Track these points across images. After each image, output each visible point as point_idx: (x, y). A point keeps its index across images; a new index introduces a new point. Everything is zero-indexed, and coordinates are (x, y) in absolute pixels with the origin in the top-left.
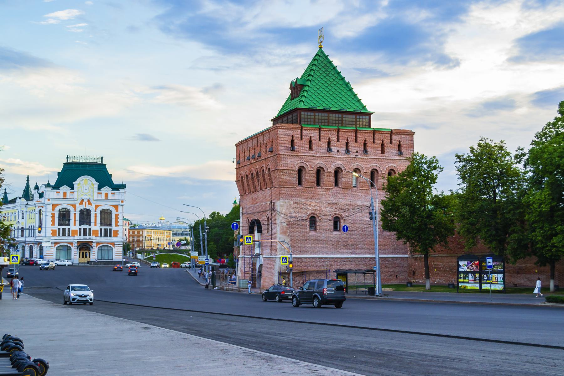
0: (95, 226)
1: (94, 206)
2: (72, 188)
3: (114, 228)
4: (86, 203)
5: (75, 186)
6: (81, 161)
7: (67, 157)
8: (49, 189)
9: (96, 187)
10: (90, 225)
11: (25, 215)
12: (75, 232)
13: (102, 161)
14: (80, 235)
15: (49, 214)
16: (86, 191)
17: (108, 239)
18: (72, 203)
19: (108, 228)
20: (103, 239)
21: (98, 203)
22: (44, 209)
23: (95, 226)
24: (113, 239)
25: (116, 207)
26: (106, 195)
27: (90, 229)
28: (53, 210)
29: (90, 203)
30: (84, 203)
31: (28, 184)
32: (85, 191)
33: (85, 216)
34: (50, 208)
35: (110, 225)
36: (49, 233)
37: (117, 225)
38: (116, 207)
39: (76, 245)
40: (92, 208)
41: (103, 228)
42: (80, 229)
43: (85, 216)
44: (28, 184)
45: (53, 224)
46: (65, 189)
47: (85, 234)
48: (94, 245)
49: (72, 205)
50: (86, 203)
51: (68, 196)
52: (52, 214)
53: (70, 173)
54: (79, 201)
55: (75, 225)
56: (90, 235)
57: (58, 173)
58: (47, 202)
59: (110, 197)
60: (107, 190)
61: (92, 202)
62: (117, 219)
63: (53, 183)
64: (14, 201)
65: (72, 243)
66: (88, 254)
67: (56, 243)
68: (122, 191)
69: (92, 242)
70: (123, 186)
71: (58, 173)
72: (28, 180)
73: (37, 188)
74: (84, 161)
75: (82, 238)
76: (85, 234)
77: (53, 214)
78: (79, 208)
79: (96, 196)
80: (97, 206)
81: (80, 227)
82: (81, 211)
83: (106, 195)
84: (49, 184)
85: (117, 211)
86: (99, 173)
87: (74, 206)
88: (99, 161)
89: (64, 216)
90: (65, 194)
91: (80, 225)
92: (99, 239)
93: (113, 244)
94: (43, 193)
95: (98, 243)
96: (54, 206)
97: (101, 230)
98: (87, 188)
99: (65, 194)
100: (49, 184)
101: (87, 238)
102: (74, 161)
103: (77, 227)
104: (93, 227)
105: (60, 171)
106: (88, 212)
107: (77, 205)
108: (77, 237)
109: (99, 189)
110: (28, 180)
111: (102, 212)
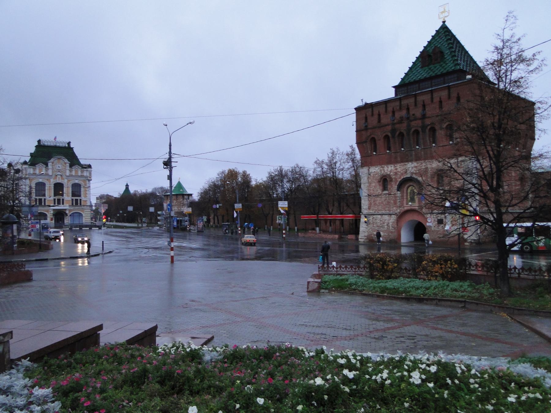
0: (67, 197)
2: (47, 165)
5: (50, 164)
7: (39, 141)
23: (67, 197)
27: (63, 199)
33: (58, 188)
35: (80, 196)
37: (86, 197)
39: (52, 212)
40: (65, 182)
43: (58, 188)
47: (59, 203)
53: (43, 153)
54: (54, 176)
56: (63, 204)
57: (31, 153)
68: (89, 169)
69: (65, 210)
70: (90, 166)
71: (31, 153)
78: (53, 181)
79: (68, 173)
83: (76, 172)
86: (67, 152)
101: (61, 207)
105: (33, 152)
109: (71, 166)
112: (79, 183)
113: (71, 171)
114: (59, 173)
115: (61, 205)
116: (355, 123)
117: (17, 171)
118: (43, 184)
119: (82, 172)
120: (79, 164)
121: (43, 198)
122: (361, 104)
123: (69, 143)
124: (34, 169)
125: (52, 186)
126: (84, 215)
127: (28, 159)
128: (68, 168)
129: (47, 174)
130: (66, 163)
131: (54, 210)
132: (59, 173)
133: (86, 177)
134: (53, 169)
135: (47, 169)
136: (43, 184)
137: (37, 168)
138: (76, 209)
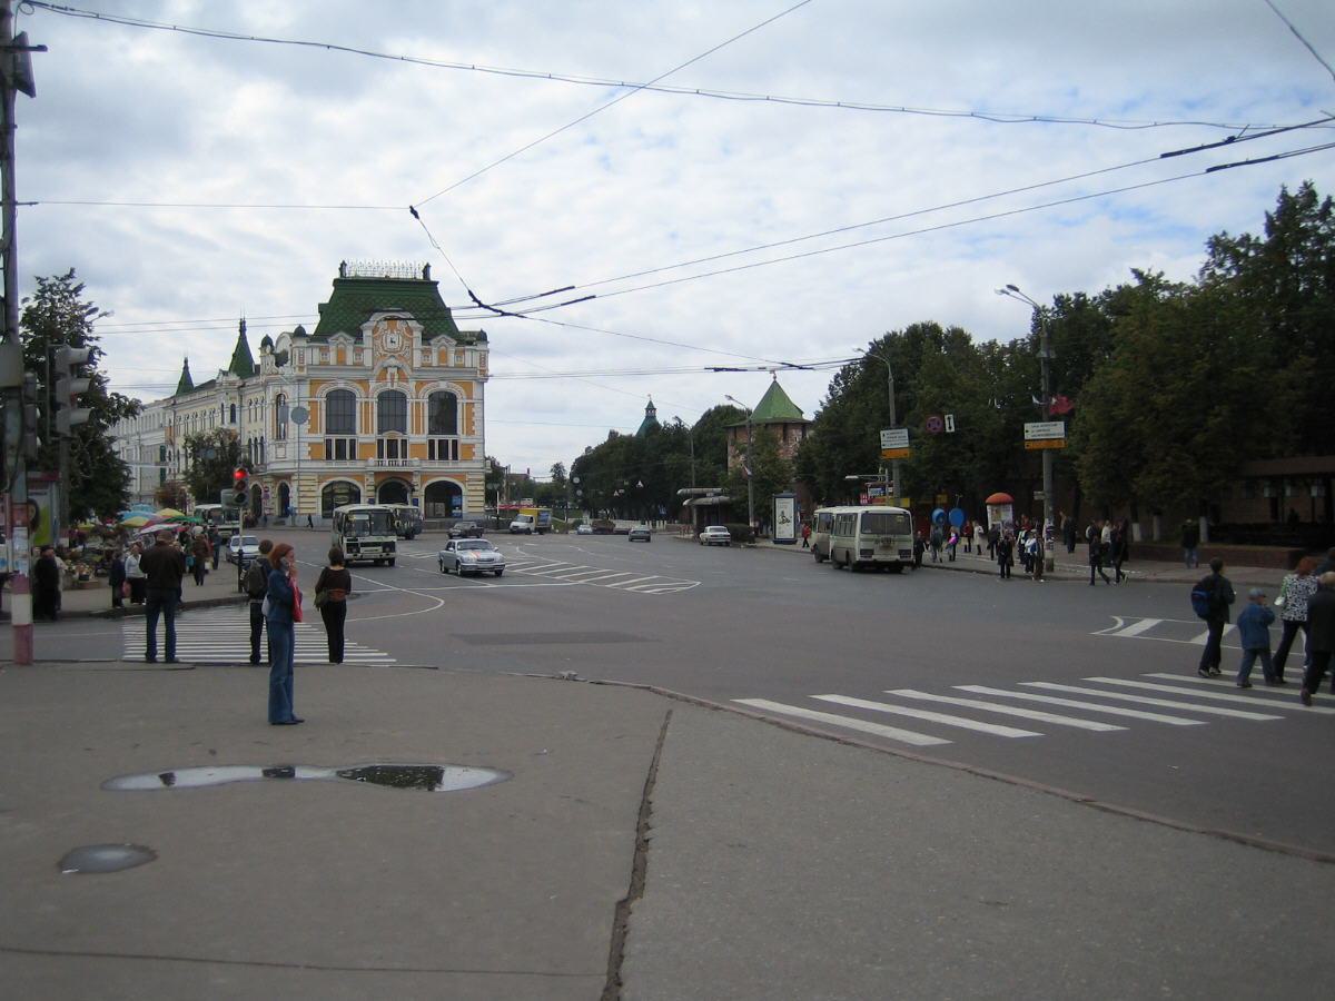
0: (418, 435)
1: (412, 384)
2: (358, 336)
3: (462, 438)
4: (393, 375)
5: (367, 334)
8: (303, 343)
9: (417, 334)
10: (403, 430)
11: (237, 414)
14: (381, 455)
16: (395, 346)
17: (449, 465)
19: (450, 438)
20: (437, 465)
24: (462, 465)
25: (468, 386)
26: (443, 356)
27: (404, 442)
29: (403, 378)
30: (388, 376)
31: (243, 338)
32: (390, 346)
33: (392, 407)
35: (454, 432)
37: (470, 432)
38: (468, 386)
40: (409, 388)
41: (436, 438)
42: (380, 442)
43: (392, 407)
44: (243, 338)
46: (341, 339)
47: (392, 454)
48: (416, 480)
49: (360, 382)
50: (393, 375)
51: (350, 358)
54: (377, 371)
55: (366, 433)
56: (404, 455)
57: (321, 306)
59: (452, 360)
60: (442, 342)
61: (407, 372)
63: (310, 330)
65: (360, 477)
68: (480, 347)
69: (410, 474)
70: (481, 337)
71: (321, 307)
72: (243, 330)
73: (267, 341)
75: (387, 465)
76: (392, 454)
78: (375, 387)
80: (420, 384)
81: (380, 437)
82: (383, 397)
83: (443, 356)
85: (470, 397)
86: (416, 299)
88: (420, 276)
89: (340, 408)
90: (341, 354)
91: (380, 432)
92: (429, 466)
93: (461, 476)
94: (285, 353)
95: (425, 476)
97: (431, 443)
99: (341, 354)
101: (398, 466)
109: (426, 338)
110: (243, 330)
114: (393, 361)
117: (281, 360)
118: (350, 397)
119: (459, 354)
120: (452, 331)
121: (348, 437)
123: (426, 269)
124: (324, 351)
125: (374, 400)
126: (463, 491)
127: (311, 325)
128: (417, 343)
129: (358, 365)
130: (410, 330)
132: (393, 361)
133: (473, 370)
135: (359, 351)
136: (349, 397)
137: (332, 348)
138: (442, 470)
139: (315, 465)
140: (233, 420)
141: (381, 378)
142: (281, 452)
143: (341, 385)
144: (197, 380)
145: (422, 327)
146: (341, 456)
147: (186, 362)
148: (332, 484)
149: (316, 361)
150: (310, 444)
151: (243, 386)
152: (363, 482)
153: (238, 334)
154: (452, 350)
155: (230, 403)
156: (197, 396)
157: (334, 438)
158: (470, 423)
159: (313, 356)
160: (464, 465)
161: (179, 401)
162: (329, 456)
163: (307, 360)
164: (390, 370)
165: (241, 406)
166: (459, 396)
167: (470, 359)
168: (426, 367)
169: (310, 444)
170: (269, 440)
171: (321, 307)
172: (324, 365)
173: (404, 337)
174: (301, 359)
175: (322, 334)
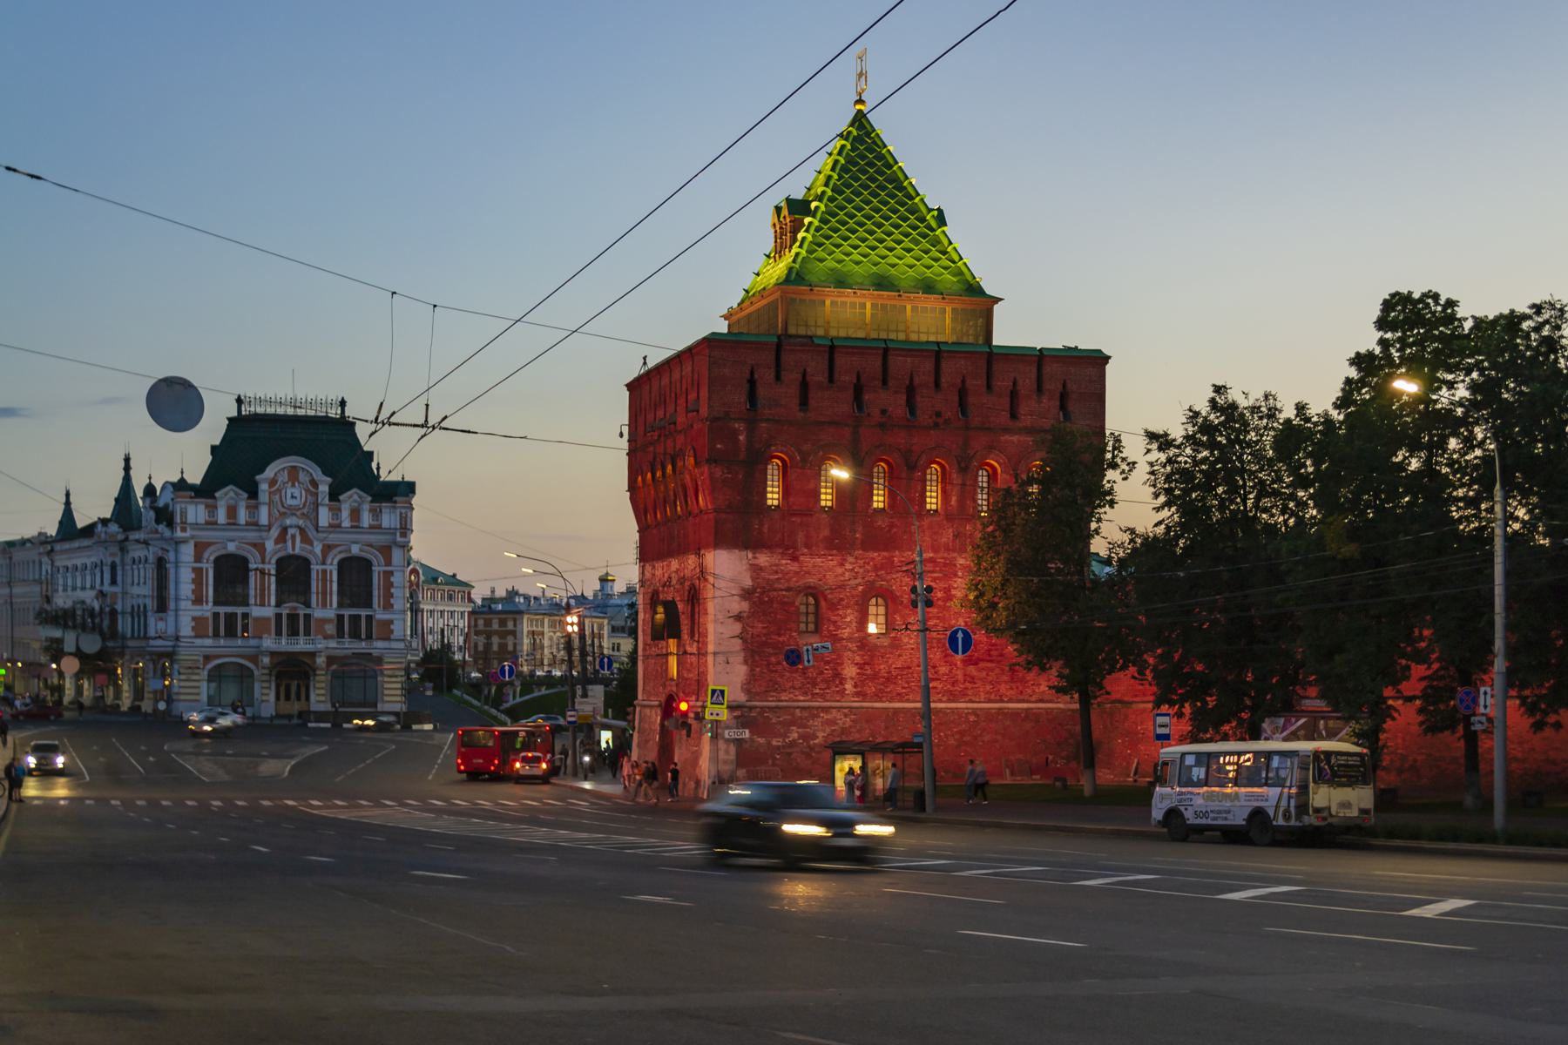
0: (325, 609)
1: (318, 549)
2: (253, 493)
5: (264, 487)
6: (280, 411)
7: (239, 401)
9: (324, 489)
10: (308, 605)
11: (119, 572)
12: (263, 621)
13: (343, 411)
14: (279, 633)
15: (186, 575)
17: (361, 646)
18: (252, 535)
19: (363, 613)
20: (350, 646)
21: (333, 538)
22: (171, 556)
26: (355, 514)
28: (198, 559)
31: (127, 479)
32: (290, 502)
34: (187, 552)
35: (369, 605)
36: (186, 629)
37: (388, 606)
38: (386, 551)
39: (266, 660)
41: (347, 613)
42: (278, 616)
44: (127, 479)
45: (198, 600)
47: (294, 632)
48: (321, 661)
49: (255, 545)
50: (293, 537)
51: (243, 516)
52: (195, 570)
54: (275, 532)
56: (307, 633)
58: (179, 534)
59: (366, 519)
61: (311, 533)
62: (389, 585)
63: (195, 477)
64: (89, 530)
66: (303, 690)
67: (207, 658)
69: (313, 655)
70: (408, 488)
71: (214, 449)
72: (127, 468)
73: (150, 490)
74: (290, 411)
75: (285, 645)
77: (198, 572)
80: (327, 549)
81: (278, 610)
82: (280, 562)
83: (355, 514)
84: (182, 480)
85: (388, 562)
87: (260, 547)
88: (334, 413)
89: (231, 574)
91: (278, 605)
95: (331, 660)
96: (200, 548)
97: (340, 618)
98: (297, 494)
99: (232, 511)
100: (182, 480)
101: (301, 645)
102: (260, 410)
103: (268, 612)
104: (318, 613)
105: (217, 443)
106: (304, 564)
107: (270, 545)
108: (269, 643)
109: (334, 496)
110: (127, 468)
111: (341, 564)
112: (363, 554)
113: (335, 511)
115: (302, 639)
116: (626, 430)
118: (245, 561)
119: (376, 513)
121: (240, 610)
122: (635, 371)
123: (343, 403)
124: (212, 509)
129: (254, 524)
130: (315, 484)
131: (273, 654)
133: (391, 531)
134: (270, 504)
135: (253, 509)
139: (199, 642)
140: (114, 582)
141: (282, 538)
142: (161, 625)
143: (231, 548)
144: (81, 522)
145: (329, 480)
146: (231, 632)
147: (68, 495)
148: (219, 666)
149: (201, 520)
150: (194, 619)
151: (126, 539)
152: (257, 665)
153: (122, 473)
154: (366, 507)
155: (109, 560)
156: (76, 544)
157: (222, 610)
158: (389, 595)
159: (196, 512)
160: (380, 644)
161: (58, 547)
162: (216, 635)
163: (191, 519)
164: (291, 531)
165: (123, 564)
166: (375, 562)
167: (389, 519)
168: (335, 527)
169: (194, 619)
170: (149, 607)
171: (214, 449)
172: (211, 524)
173: (307, 490)
174: (184, 514)
175: (205, 490)
